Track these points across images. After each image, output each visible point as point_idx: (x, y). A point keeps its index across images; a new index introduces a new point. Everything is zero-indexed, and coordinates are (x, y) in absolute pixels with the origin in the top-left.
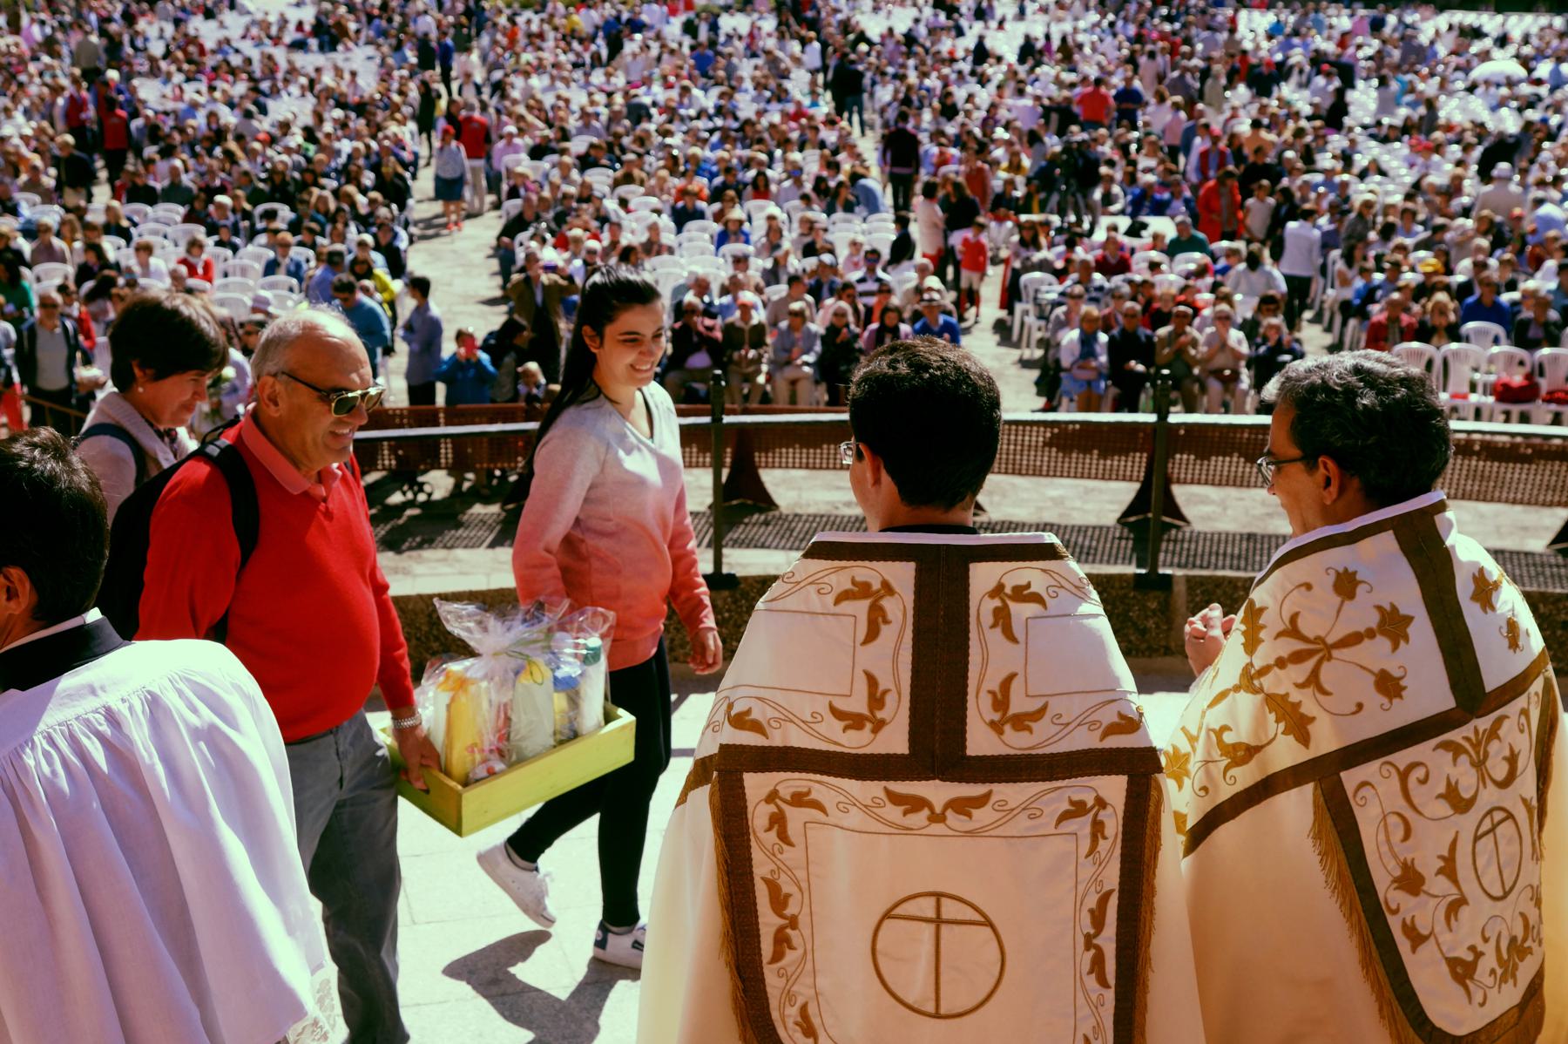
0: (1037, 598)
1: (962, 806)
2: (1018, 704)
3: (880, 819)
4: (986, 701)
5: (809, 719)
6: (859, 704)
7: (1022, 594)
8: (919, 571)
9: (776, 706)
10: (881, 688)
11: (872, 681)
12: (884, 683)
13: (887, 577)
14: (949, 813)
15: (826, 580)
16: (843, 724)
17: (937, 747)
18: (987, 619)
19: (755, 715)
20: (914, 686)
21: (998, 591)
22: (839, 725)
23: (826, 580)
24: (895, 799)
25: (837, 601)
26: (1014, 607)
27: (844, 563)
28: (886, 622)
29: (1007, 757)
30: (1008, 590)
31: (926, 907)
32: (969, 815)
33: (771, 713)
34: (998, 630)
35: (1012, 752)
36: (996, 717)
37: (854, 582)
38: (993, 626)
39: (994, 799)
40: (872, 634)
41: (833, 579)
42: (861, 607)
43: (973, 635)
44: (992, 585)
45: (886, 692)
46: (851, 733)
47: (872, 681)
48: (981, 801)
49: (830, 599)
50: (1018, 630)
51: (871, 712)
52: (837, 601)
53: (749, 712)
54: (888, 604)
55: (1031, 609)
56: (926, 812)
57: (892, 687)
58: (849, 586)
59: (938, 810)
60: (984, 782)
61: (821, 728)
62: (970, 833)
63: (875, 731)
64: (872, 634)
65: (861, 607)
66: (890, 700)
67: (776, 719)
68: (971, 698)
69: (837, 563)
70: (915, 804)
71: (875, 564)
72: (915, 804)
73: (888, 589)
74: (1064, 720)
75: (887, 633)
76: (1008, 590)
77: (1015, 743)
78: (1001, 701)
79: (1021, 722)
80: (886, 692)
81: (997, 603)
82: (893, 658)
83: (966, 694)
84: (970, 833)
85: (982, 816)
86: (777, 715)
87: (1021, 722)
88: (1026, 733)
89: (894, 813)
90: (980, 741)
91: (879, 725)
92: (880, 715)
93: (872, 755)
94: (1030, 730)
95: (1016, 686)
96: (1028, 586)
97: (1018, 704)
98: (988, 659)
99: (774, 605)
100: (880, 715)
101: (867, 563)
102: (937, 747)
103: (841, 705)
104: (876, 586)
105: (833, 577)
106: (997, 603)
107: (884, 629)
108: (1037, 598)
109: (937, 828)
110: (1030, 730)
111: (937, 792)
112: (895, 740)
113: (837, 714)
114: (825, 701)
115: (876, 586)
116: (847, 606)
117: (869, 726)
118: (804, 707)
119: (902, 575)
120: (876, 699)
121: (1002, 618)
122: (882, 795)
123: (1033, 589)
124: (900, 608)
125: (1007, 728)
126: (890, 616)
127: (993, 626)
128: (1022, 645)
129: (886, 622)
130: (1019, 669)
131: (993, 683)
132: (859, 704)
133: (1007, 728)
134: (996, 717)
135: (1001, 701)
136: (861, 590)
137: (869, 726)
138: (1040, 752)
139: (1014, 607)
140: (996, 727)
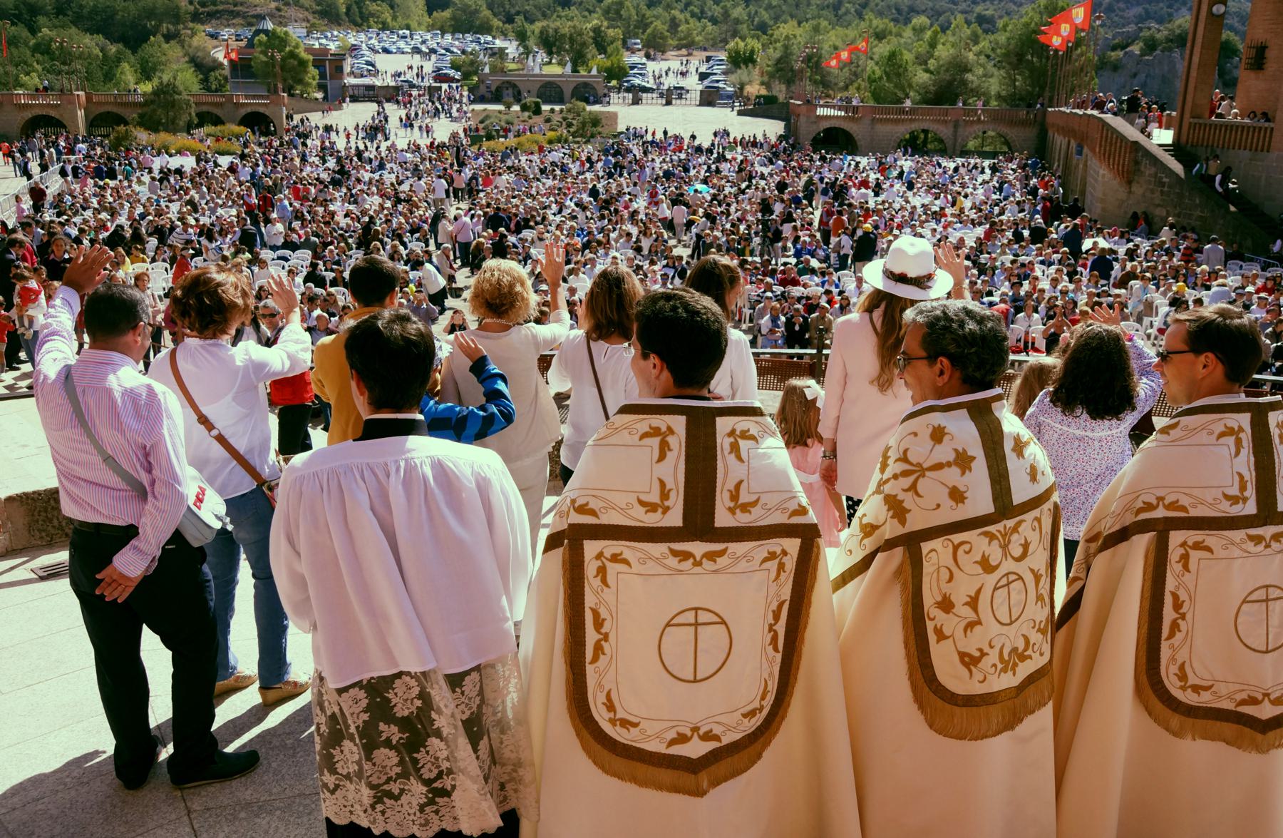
0: (753, 438)
1: (711, 556)
2: (744, 498)
3: (665, 566)
4: (726, 495)
6: (654, 498)
7: (745, 435)
8: (688, 421)
11: (662, 484)
14: (704, 560)
18: (727, 447)
19: (591, 506)
21: (732, 433)
22: (644, 509)
24: (675, 553)
25: (641, 438)
26: (742, 443)
29: (737, 528)
31: (690, 618)
33: (602, 504)
36: (732, 505)
40: (662, 457)
41: (638, 426)
42: (655, 442)
43: (719, 457)
44: (729, 430)
46: (650, 515)
47: (662, 484)
49: (637, 437)
50: (744, 455)
52: (641, 438)
53: (587, 504)
54: (670, 439)
55: (750, 443)
56: (691, 560)
58: (647, 429)
62: (715, 572)
64: (662, 457)
65: (655, 442)
66: (673, 495)
68: (718, 494)
70: (686, 556)
71: (663, 417)
72: (686, 556)
73: (671, 431)
75: (671, 456)
77: (742, 520)
78: (735, 496)
81: (732, 440)
82: (674, 470)
83: (715, 491)
84: (715, 572)
85: (722, 561)
87: (745, 508)
89: (673, 562)
90: (723, 519)
91: (666, 510)
92: (666, 503)
95: (744, 487)
97: (744, 498)
98: (728, 471)
100: (666, 503)
103: (644, 498)
104: (664, 429)
106: (732, 440)
107: (669, 454)
108: (753, 438)
109: (698, 569)
111: (698, 548)
112: (675, 518)
113: (642, 503)
115: (664, 429)
116: (647, 441)
117: (660, 510)
118: (620, 500)
119: (679, 423)
120: (665, 495)
121: (735, 448)
122: (667, 551)
125: (738, 511)
126: (672, 447)
131: (731, 485)
132: (654, 498)
133: (738, 511)
134: (732, 505)
135: (735, 496)
136: (655, 432)
137: (660, 510)
139: (742, 443)
140: (732, 511)
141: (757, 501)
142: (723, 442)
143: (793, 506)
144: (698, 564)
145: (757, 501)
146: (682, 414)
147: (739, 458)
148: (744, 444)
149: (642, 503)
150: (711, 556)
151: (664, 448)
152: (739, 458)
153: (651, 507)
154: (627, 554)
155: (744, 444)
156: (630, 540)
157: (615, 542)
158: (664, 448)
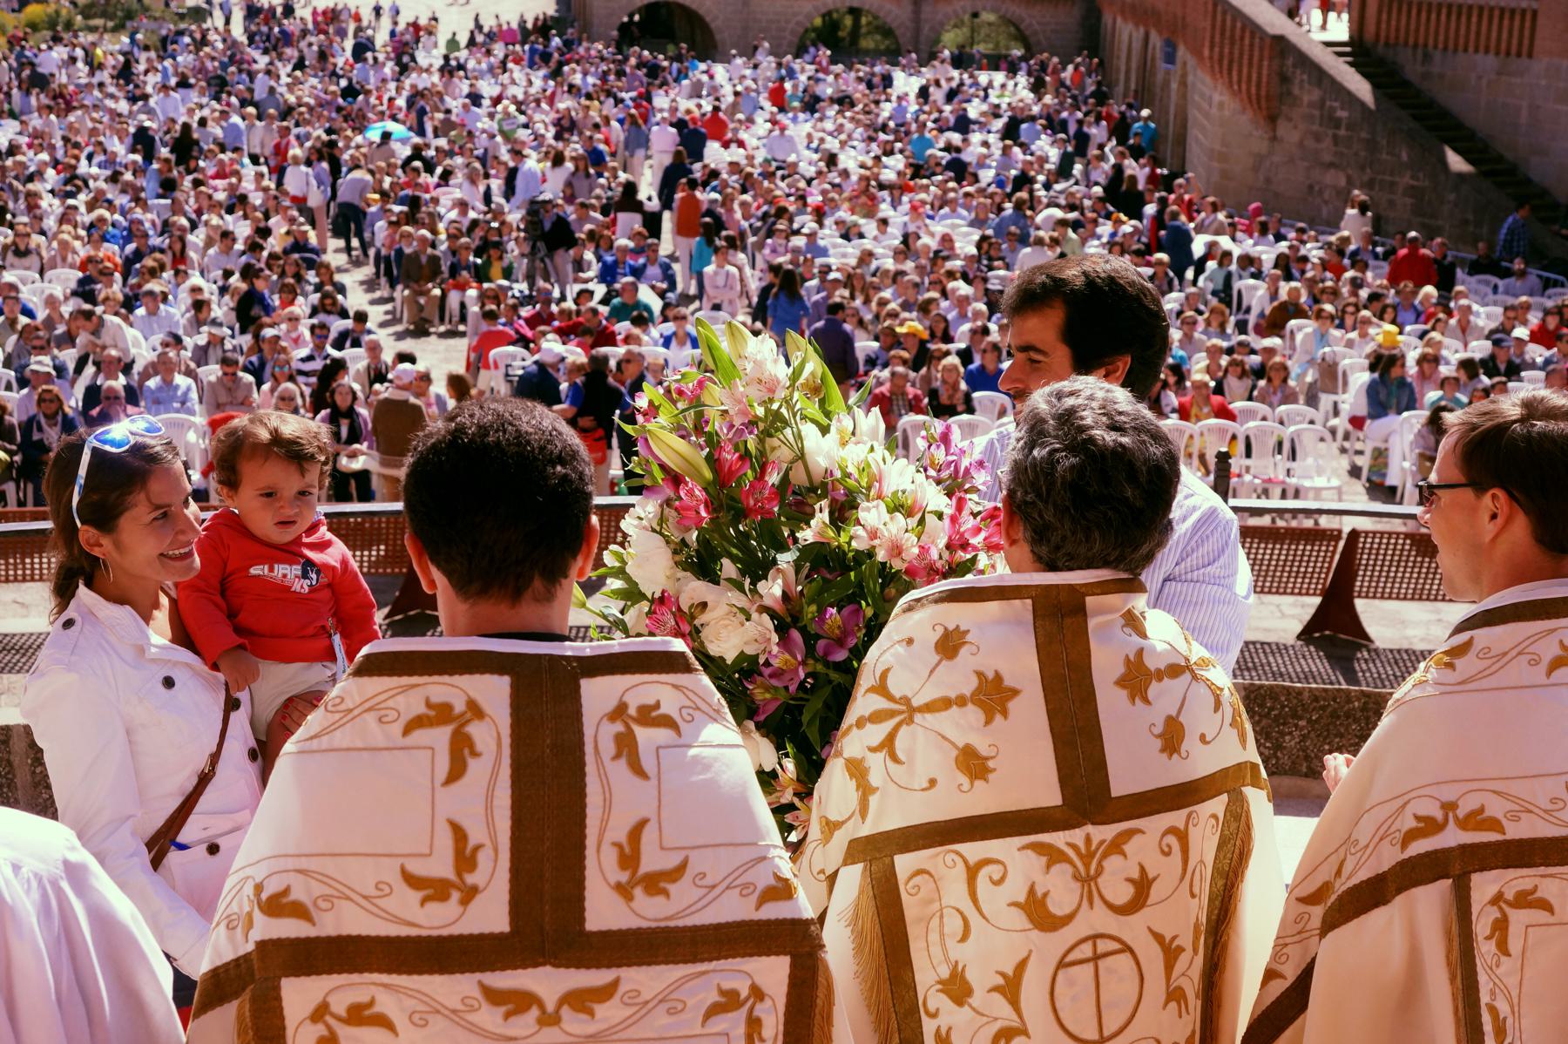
0: (668, 722)
1: (581, 1001)
2: (652, 860)
4: (610, 857)
5: (372, 892)
6: (441, 866)
7: (650, 716)
9: (324, 878)
10: (472, 842)
12: (476, 834)
13: (475, 695)
14: (566, 1012)
15: (390, 703)
16: (419, 895)
17: (547, 921)
18: (608, 748)
19: (297, 894)
20: (515, 839)
21: (619, 712)
22: (415, 896)
23: (390, 703)
24: (494, 997)
25: (407, 731)
27: (415, 680)
28: (475, 754)
29: (637, 933)
30: (632, 711)
32: (591, 1013)
33: (318, 889)
34: (622, 763)
35: (645, 924)
36: (624, 877)
37: (429, 705)
38: (617, 756)
39: (622, 989)
40: (457, 771)
41: (400, 701)
42: (440, 737)
44: (611, 704)
45: (477, 848)
46: (433, 907)
48: (606, 993)
49: (397, 728)
50: (648, 763)
51: (459, 874)
52: (407, 731)
53: (286, 891)
54: (476, 730)
55: (662, 735)
56: (535, 1012)
57: (488, 843)
58: (421, 709)
59: (550, 1007)
60: (609, 966)
61: (388, 904)
63: (465, 901)
64: (457, 771)
65: (440, 737)
66: (484, 858)
67: (325, 898)
68: (590, 852)
69: (405, 680)
70: (519, 1002)
71: (458, 680)
72: (519, 1002)
74: (708, 881)
75: (477, 769)
76: (632, 711)
77: (649, 912)
78: (629, 857)
79: (655, 883)
80: (477, 848)
81: (619, 727)
82: (486, 801)
83: (583, 847)
86: (329, 891)
87: (655, 883)
88: (660, 899)
90: (604, 911)
91: (469, 894)
92: (470, 879)
93: (461, 937)
94: (666, 893)
95: (649, 837)
96: (657, 705)
97: (652, 860)
98: (611, 800)
99: (315, 744)
100: (470, 879)
101: (446, 678)
102: (547, 921)
103: (418, 868)
104: (459, 706)
105: (400, 698)
107: (473, 764)
108: (668, 722)
110: (666, 893)
111: (547, 982)
112: (490, 913)
113: (412, 881)
114: (395, 864)
115: (459, 706)
116: (421, 736)
117: (456, 896)
118: (363, 876)
119: (494, 691)
120: (465, 858)
121: (626, 746)
122: (476, 993)
123: (663, 710)
124: (493, 735)
125: (638, 892)
126: (479, 747)
127: (617, 756)
128: (654, 782)
129: (475, 754)
130: (648, 811)
132: (441, 866)
133: (638, 892)
134: (624, 877)
135: (629, 857)
136: (440, 714)
137: (456, 896)
138: (680, 923)
140: (624, 890)
141: (681, 869)
142: (598, 734)
143: (764, 880)
144: (550, 1020)
145: (681, 869)
146: (500, 671)
147: (638, 770)
148: (646, 737)
149: (412, 881)
150: (581, 1001)
151: (461, 752)
152: (638, 770)
153: (435, 890)
154: (386, 1004)
155: (646, 737)
156: (390, 971)
157: (355, 977)
158: (461, 752)
